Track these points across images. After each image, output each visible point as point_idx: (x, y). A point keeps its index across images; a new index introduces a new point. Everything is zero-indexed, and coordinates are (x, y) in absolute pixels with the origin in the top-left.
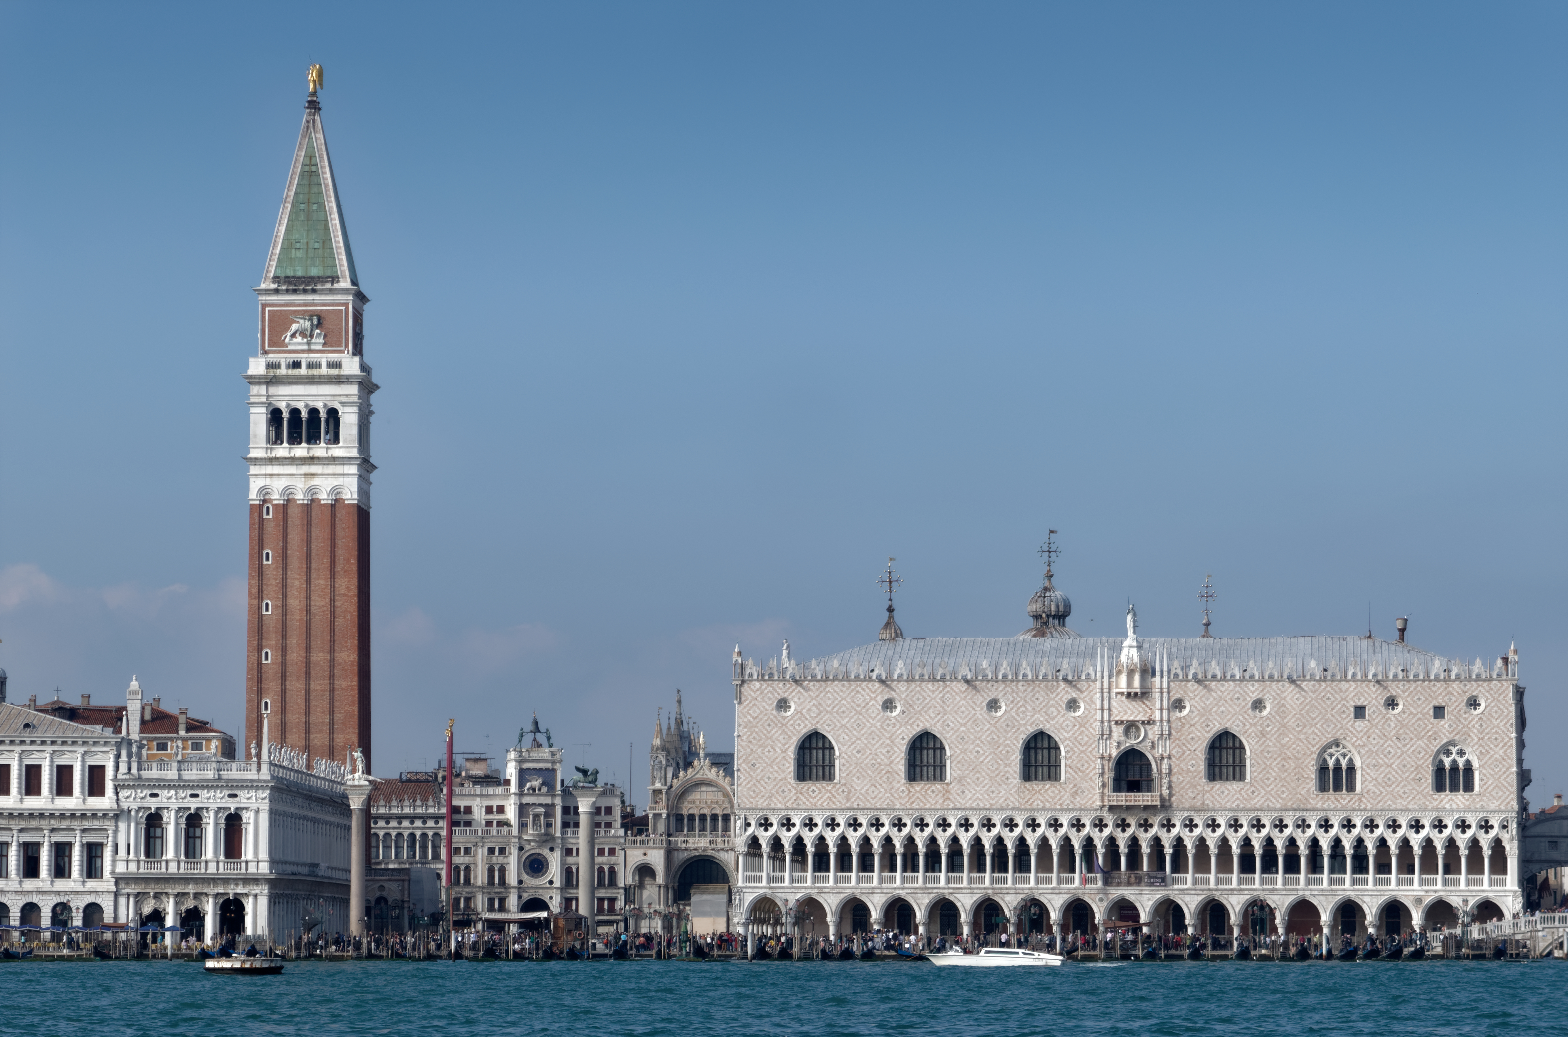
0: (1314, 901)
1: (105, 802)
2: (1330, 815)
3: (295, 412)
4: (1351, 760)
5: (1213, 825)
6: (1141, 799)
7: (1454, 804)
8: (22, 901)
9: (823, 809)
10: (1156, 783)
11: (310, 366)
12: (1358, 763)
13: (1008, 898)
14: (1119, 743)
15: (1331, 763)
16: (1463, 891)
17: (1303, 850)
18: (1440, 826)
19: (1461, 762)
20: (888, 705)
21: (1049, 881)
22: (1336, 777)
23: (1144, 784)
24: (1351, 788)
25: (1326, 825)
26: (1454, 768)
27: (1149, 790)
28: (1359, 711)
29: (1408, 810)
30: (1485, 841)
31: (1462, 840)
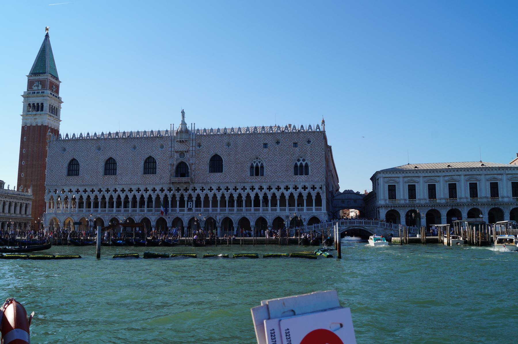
0: (248, 217)
2: (254, 184)
4: (262, 164)
5: (211, 189)
6: (184, 179)
7: (301, 180)
10: (190, 174)
12: (264, 165)
13: (136, 217)
14: (177, 160)
15: (255, 165)
16: (305, 213)
17: (244, 198)
18: (296, 188)
19: (304, 163)
21: (151, 211)
22: (257, 171)
23: (186, 175)
25: (253, 189)
28: (265, 145)
29: (283, 182)
30: (314, 194)
31: (305, 194)
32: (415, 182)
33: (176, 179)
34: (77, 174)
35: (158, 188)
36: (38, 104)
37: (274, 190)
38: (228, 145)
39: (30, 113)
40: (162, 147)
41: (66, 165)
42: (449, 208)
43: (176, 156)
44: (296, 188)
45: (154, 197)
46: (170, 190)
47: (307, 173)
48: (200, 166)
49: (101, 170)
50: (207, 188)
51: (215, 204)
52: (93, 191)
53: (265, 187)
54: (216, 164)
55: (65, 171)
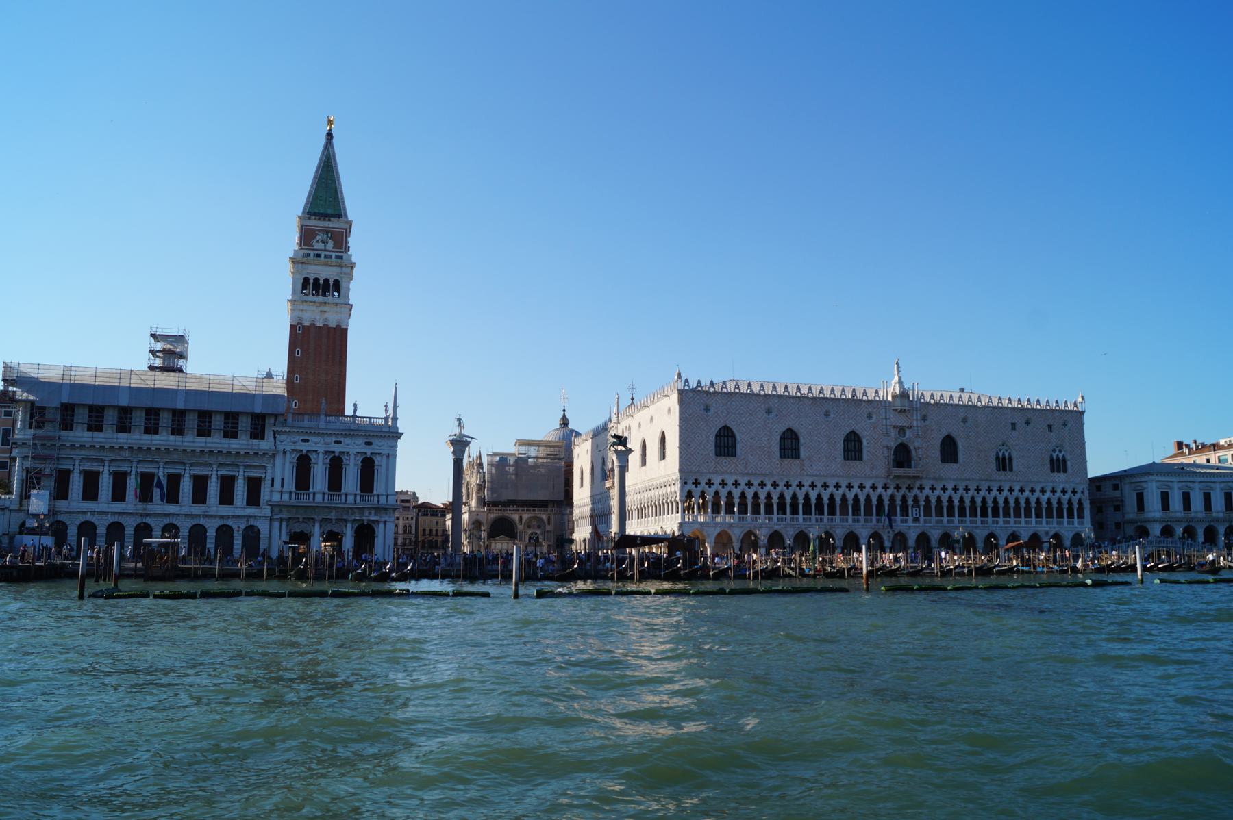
1: (265, 445)
3: (316, 280)
5: (944, 489)
6: (911, 472)
8: (190, 523)
9: (731, 473)
11: (326, 256)
12: (1014, 455)
16: (1067, 529)
19: (1061, 456)
20: (769, 412)
21: (859, 521)
22: (1004, 464)
24: (1011, 470)
26: (1058, 459)
27: (909, 466)
28: (1014, 425)
32: (1189, 488)
33: (900, 472)
34: (732, 453)
35: (868, 485)
36: (326, 281)
37: (1027, 493)
38: (965, 420)
39: (310, 298)
40: (870, 416)
41: (712, 438)
42: (1227, 525)
43: (893, 433)
44: (1054, 491)
45: (862, 499)
46: (885, 487)
47: (1065, 471)
48: (927, 451)
49: (776, 449)
50: (939, 486)
51: (807, 511)
52: (762, 485)
53: (1017, 488)
54: (949, 450)
55: (712, 447)
